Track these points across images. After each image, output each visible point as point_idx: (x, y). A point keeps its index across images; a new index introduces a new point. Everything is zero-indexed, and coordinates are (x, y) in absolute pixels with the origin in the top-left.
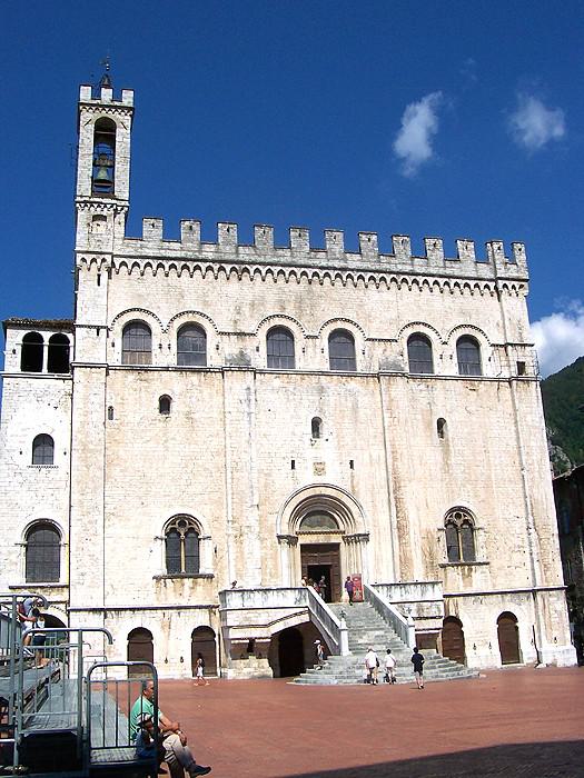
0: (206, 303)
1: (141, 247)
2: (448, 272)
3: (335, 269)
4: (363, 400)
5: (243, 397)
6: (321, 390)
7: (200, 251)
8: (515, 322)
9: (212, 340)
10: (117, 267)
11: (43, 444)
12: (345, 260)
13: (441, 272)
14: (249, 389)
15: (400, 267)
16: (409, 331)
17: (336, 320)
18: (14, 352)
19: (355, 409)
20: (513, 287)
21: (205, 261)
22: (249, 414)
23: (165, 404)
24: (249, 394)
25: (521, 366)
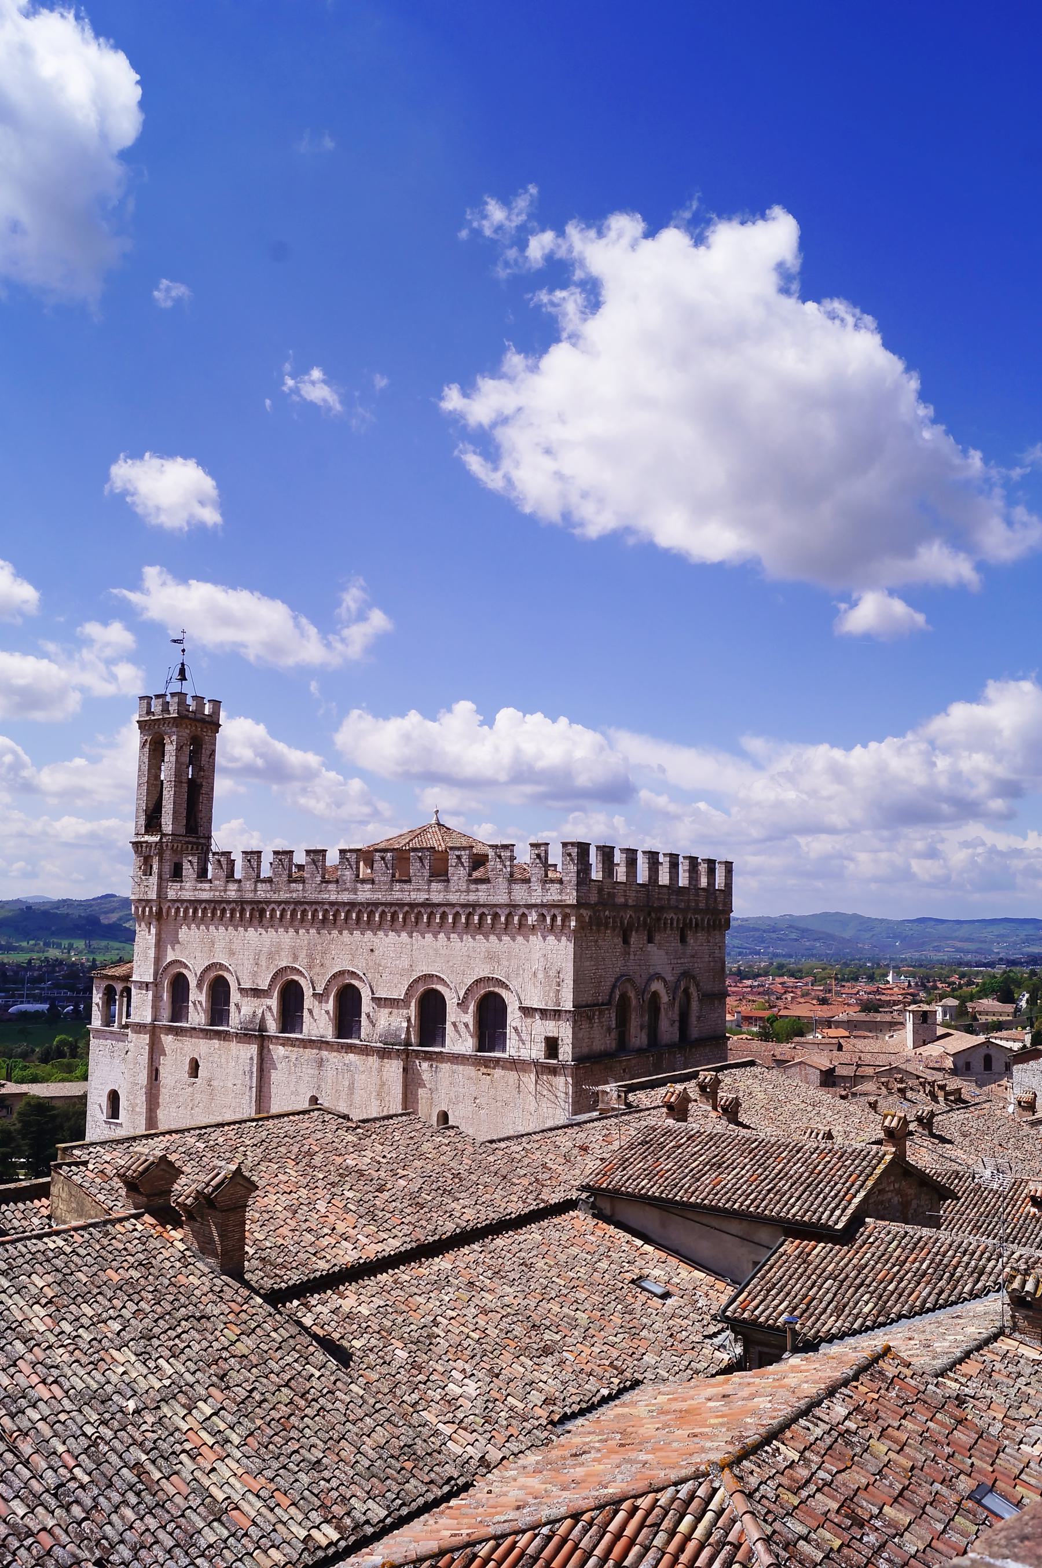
0: (232, 953)
1: (181, 889)
2: (472, 898)
3: (344, 904)
4: (361, 1079)
5: (247, 1069)
6: (321, 1063)
7: (225, 891)
8: (552, 973)
9: (235, 996)
10: (164, 910)
11: (114, 1097)
12: (355, 891)
13: (463, 898)
14: (251, 1059)
15: (414, 895)
16: (421, 989)
17: (341, 973)
18: (97, 1004)
19: (351, 1088)
20: (554, 918)
21: (229, 902)
22: (251, 1088)
23: (194, 1068)
24: (252, 1064)
25: (552, 1045)
